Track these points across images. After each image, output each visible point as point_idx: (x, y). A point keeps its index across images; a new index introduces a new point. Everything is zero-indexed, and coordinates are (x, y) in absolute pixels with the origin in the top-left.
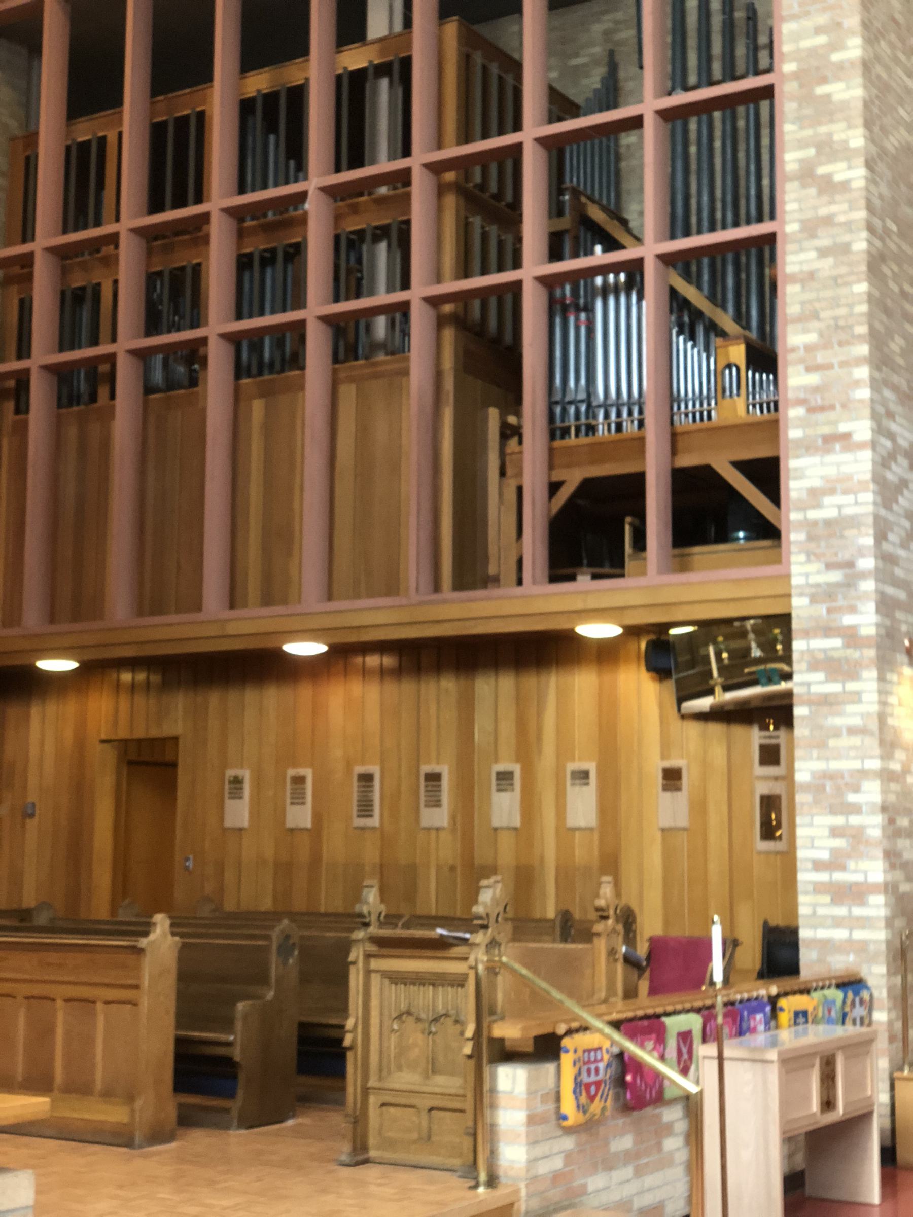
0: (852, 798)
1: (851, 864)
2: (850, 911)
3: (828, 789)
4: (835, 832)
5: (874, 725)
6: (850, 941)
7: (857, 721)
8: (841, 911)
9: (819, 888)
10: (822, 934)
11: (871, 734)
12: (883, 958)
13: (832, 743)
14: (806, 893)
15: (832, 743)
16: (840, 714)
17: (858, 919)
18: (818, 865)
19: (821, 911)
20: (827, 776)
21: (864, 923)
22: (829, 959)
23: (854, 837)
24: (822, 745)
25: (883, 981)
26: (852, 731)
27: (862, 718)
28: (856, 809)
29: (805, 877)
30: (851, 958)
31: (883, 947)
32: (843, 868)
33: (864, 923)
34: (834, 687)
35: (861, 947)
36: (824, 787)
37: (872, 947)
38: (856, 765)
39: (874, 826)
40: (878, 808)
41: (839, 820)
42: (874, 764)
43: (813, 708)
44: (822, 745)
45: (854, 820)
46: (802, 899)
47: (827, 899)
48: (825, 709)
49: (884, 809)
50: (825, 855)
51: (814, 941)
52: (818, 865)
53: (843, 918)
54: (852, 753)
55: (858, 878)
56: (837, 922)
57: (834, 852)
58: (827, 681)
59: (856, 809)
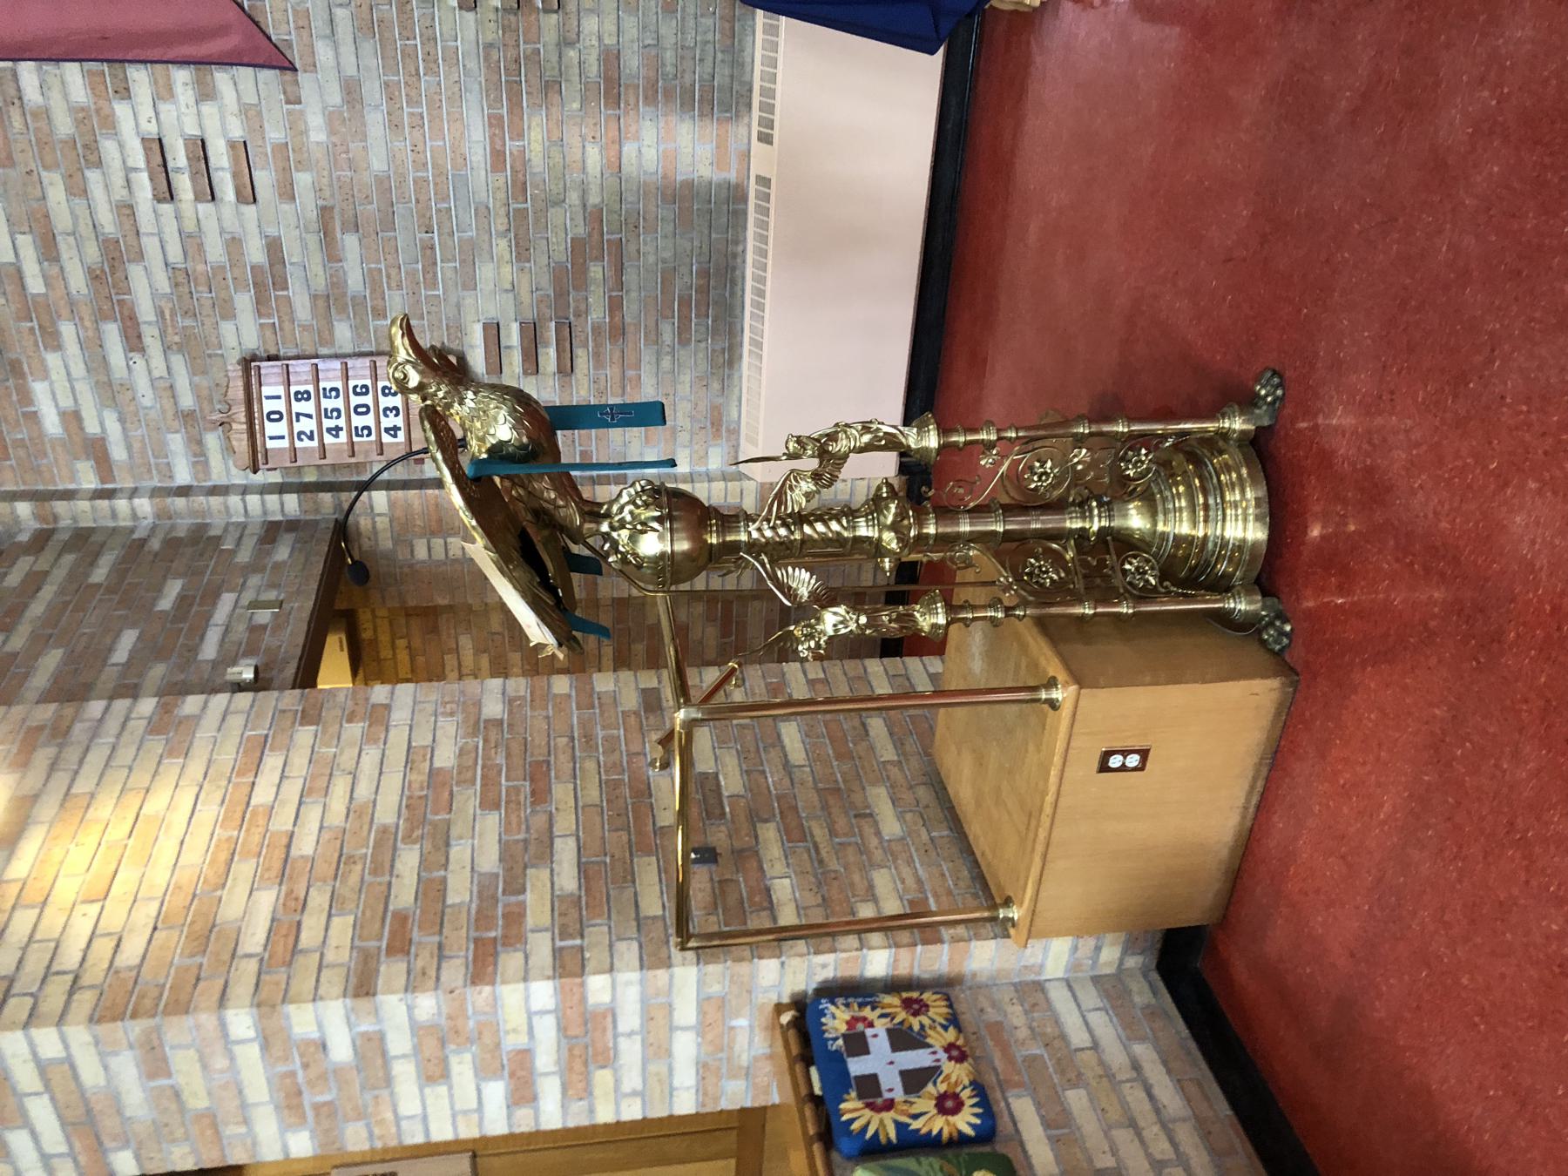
0: (341, 1050)
1: (513, 1041)
2: (630, 1034)
3: (327, 1097)
4: (435, 1072)
5: (136, 1028)
6: (702, 1028)
7: (127, 1068)
8: (630, 1051)
9: (576, 1082)
10: (685, 1077)
11: (158, 1029)
12: (743, 968)
13: (198, 1101)
14: (592, 1111)
15: (198, 1101)
16: (115, 1100)
17: (647, 1017)
18: (523, 1092)
19: (632, 1080)
20: (290, 1103)
21: (657, 1015)
22: (744, 1060)
23: (443, 1043)
24: (211, 1120)
25: (795, 963)
26: (155, 1062)
27: (116, 1054)
28: (372, 1049)
29: (551, 1113)
30: (742, 1022)
31: (714, 969)
32: (524, 1057)
33: (657, 1015)
34: (42, 1112)
35: (713, 1012)
36: (317, 1108)
37: (715, 989)
38: (250, 1057)
39: (410, 1008)
40: (364, 1003)
41: (405, 1073)
42: (241, 1022)
43: (108, 1144)
44: (211, 1120)
45: (399, 1042)
46: (605, 1115)
47: (602, 1078)
48: (109, 1124)
49: (363, 986)
50: (496, 1092)
51: (702, 1088)
52: (523, 1092)
53: (645, 1044)
54: (220, 1063)
55: (547, 1030)
56: (657, 1050)
57: (483, 1072)
58: (26, 1123)
59: (372, 1049)
